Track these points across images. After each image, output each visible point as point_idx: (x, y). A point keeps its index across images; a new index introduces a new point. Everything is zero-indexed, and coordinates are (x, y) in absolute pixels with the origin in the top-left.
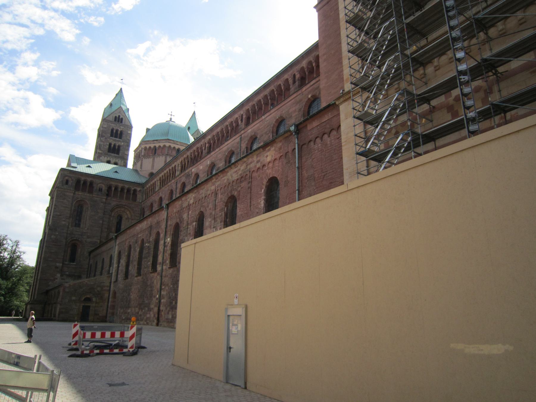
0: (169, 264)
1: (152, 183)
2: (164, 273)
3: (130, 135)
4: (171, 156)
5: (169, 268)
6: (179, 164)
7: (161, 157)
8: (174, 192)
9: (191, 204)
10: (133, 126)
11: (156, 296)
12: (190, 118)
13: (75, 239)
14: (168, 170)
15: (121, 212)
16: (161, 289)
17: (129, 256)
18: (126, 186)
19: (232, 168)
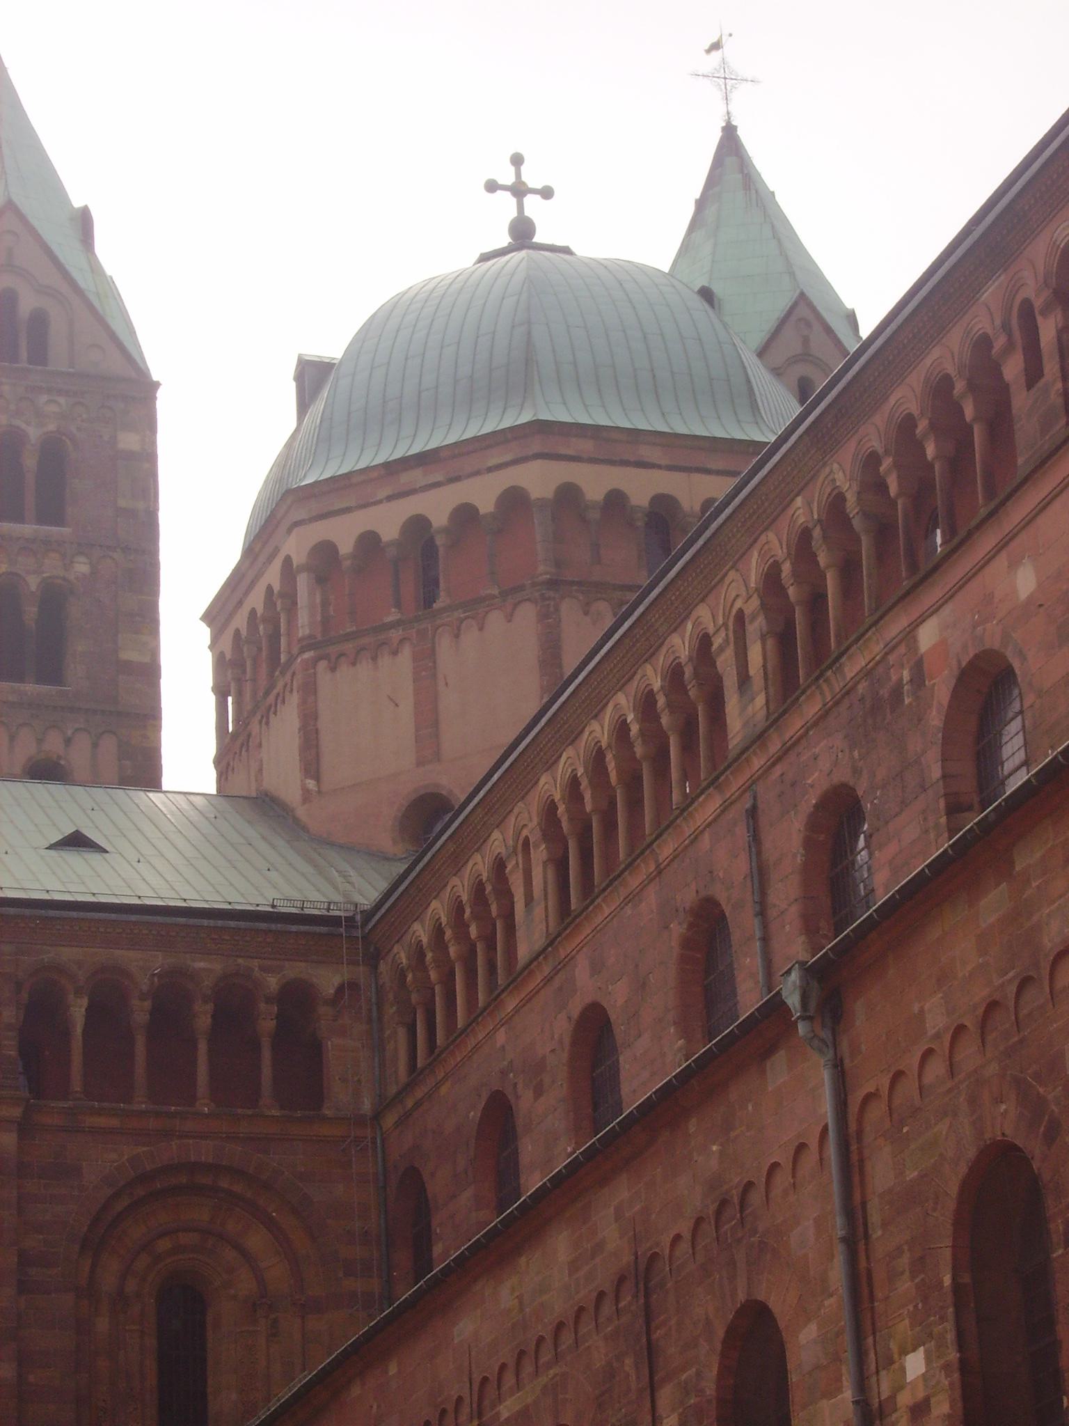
1: (460, 886)
6: (740, 617)
7: (495, 619)
8: (743, 924)
10: (157, 365)
12: (701, 204)
14: (623, 703)
18: (202, 965)
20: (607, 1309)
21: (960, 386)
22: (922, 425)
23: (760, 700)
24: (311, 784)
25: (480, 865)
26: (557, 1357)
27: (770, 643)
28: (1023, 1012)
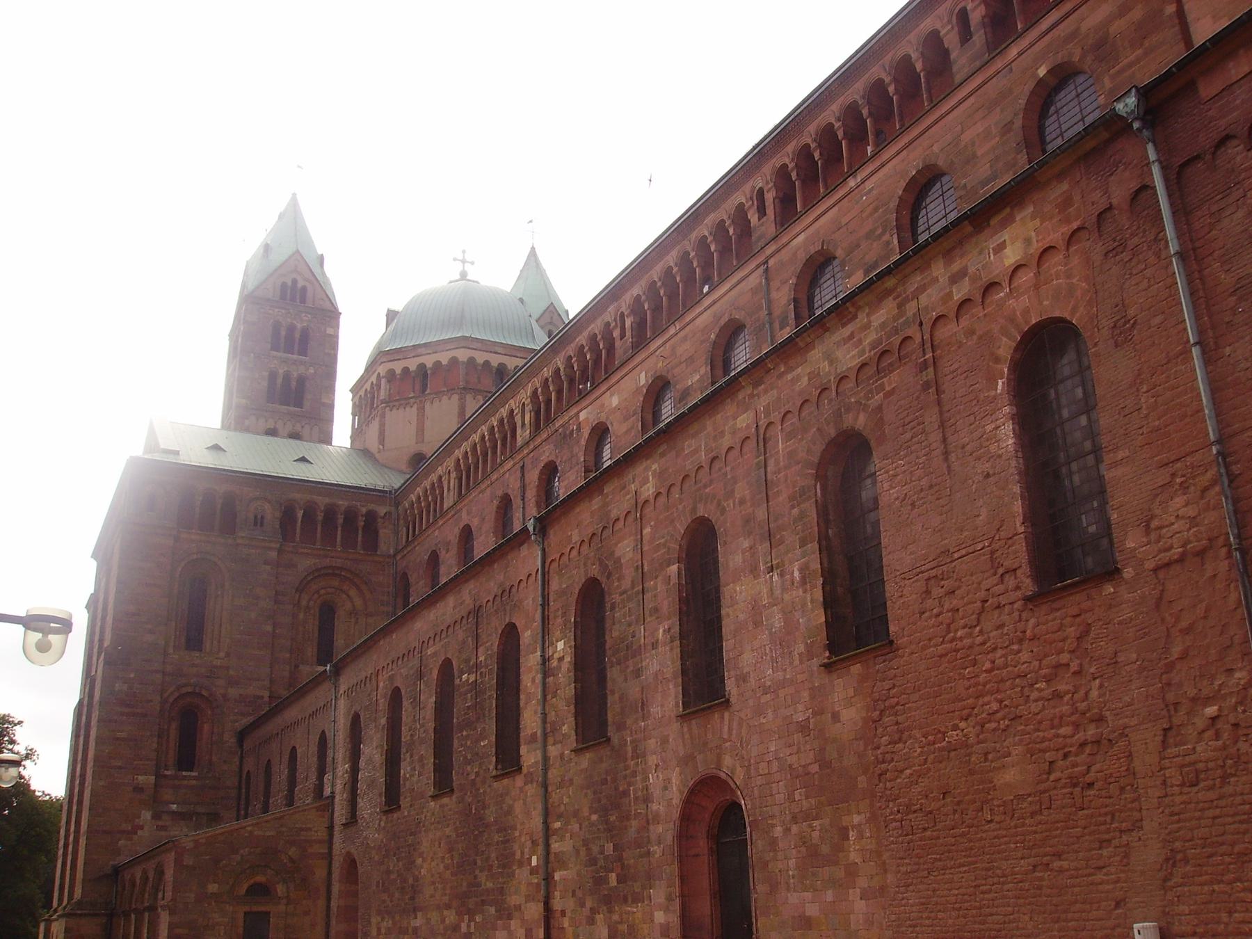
0: (573, 737)
1: (427, 484)
2: (553, 774)
3: (331, 344)
4: (476, 391)
5: (576, 751)
8: (517, 502)
9: (646, 502)
11: (530, 859)
13: (190, 689)
14: (484, 429)
15: (330, 590)
16: (548, 832)
17: (394, 728)
18: (341, 503)
19: (827, 330)
20: (464, 621)
21: (599, 337)
22: (587, 348)
23: (528, 432)
24: (381, 447)
25: (434, 477)
26: (447, 636)
27: (532, 414)
28: (603, 537)
